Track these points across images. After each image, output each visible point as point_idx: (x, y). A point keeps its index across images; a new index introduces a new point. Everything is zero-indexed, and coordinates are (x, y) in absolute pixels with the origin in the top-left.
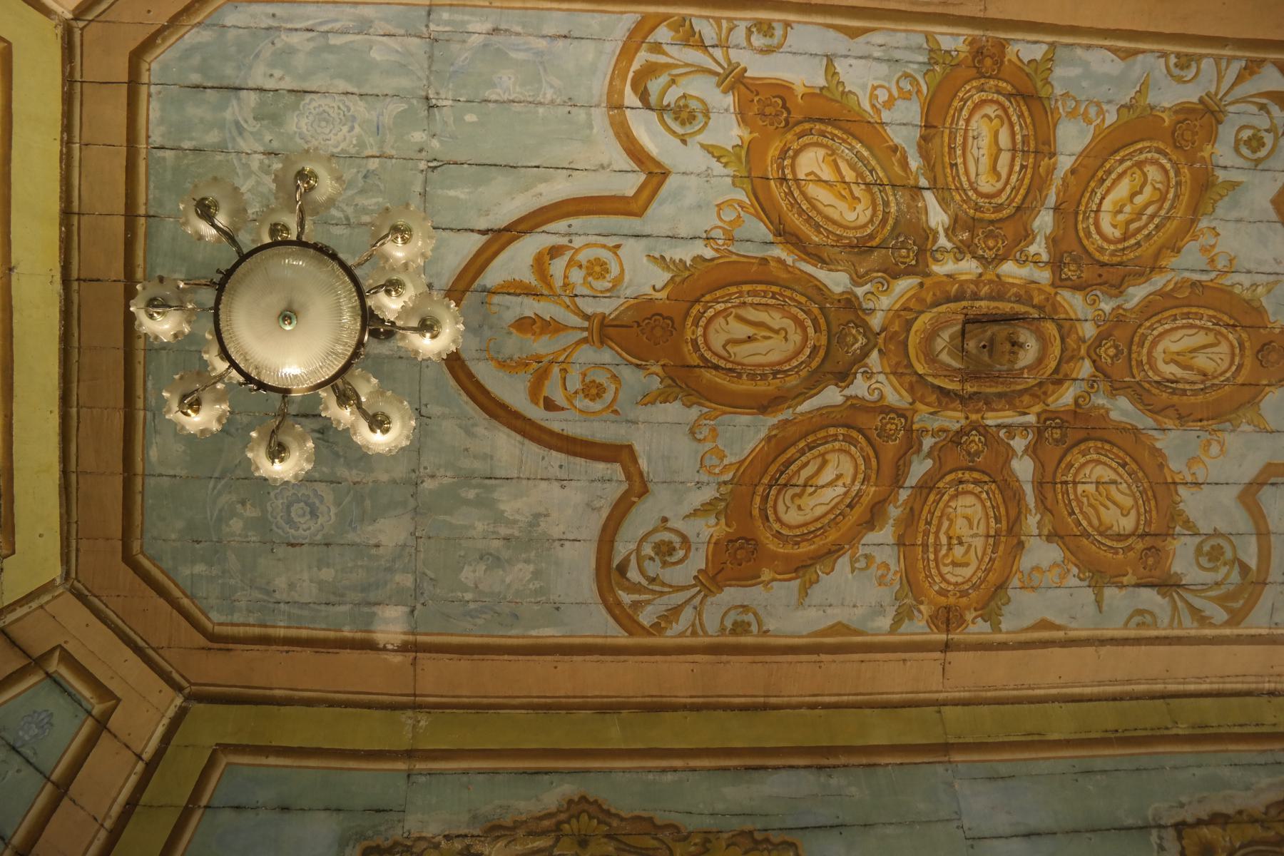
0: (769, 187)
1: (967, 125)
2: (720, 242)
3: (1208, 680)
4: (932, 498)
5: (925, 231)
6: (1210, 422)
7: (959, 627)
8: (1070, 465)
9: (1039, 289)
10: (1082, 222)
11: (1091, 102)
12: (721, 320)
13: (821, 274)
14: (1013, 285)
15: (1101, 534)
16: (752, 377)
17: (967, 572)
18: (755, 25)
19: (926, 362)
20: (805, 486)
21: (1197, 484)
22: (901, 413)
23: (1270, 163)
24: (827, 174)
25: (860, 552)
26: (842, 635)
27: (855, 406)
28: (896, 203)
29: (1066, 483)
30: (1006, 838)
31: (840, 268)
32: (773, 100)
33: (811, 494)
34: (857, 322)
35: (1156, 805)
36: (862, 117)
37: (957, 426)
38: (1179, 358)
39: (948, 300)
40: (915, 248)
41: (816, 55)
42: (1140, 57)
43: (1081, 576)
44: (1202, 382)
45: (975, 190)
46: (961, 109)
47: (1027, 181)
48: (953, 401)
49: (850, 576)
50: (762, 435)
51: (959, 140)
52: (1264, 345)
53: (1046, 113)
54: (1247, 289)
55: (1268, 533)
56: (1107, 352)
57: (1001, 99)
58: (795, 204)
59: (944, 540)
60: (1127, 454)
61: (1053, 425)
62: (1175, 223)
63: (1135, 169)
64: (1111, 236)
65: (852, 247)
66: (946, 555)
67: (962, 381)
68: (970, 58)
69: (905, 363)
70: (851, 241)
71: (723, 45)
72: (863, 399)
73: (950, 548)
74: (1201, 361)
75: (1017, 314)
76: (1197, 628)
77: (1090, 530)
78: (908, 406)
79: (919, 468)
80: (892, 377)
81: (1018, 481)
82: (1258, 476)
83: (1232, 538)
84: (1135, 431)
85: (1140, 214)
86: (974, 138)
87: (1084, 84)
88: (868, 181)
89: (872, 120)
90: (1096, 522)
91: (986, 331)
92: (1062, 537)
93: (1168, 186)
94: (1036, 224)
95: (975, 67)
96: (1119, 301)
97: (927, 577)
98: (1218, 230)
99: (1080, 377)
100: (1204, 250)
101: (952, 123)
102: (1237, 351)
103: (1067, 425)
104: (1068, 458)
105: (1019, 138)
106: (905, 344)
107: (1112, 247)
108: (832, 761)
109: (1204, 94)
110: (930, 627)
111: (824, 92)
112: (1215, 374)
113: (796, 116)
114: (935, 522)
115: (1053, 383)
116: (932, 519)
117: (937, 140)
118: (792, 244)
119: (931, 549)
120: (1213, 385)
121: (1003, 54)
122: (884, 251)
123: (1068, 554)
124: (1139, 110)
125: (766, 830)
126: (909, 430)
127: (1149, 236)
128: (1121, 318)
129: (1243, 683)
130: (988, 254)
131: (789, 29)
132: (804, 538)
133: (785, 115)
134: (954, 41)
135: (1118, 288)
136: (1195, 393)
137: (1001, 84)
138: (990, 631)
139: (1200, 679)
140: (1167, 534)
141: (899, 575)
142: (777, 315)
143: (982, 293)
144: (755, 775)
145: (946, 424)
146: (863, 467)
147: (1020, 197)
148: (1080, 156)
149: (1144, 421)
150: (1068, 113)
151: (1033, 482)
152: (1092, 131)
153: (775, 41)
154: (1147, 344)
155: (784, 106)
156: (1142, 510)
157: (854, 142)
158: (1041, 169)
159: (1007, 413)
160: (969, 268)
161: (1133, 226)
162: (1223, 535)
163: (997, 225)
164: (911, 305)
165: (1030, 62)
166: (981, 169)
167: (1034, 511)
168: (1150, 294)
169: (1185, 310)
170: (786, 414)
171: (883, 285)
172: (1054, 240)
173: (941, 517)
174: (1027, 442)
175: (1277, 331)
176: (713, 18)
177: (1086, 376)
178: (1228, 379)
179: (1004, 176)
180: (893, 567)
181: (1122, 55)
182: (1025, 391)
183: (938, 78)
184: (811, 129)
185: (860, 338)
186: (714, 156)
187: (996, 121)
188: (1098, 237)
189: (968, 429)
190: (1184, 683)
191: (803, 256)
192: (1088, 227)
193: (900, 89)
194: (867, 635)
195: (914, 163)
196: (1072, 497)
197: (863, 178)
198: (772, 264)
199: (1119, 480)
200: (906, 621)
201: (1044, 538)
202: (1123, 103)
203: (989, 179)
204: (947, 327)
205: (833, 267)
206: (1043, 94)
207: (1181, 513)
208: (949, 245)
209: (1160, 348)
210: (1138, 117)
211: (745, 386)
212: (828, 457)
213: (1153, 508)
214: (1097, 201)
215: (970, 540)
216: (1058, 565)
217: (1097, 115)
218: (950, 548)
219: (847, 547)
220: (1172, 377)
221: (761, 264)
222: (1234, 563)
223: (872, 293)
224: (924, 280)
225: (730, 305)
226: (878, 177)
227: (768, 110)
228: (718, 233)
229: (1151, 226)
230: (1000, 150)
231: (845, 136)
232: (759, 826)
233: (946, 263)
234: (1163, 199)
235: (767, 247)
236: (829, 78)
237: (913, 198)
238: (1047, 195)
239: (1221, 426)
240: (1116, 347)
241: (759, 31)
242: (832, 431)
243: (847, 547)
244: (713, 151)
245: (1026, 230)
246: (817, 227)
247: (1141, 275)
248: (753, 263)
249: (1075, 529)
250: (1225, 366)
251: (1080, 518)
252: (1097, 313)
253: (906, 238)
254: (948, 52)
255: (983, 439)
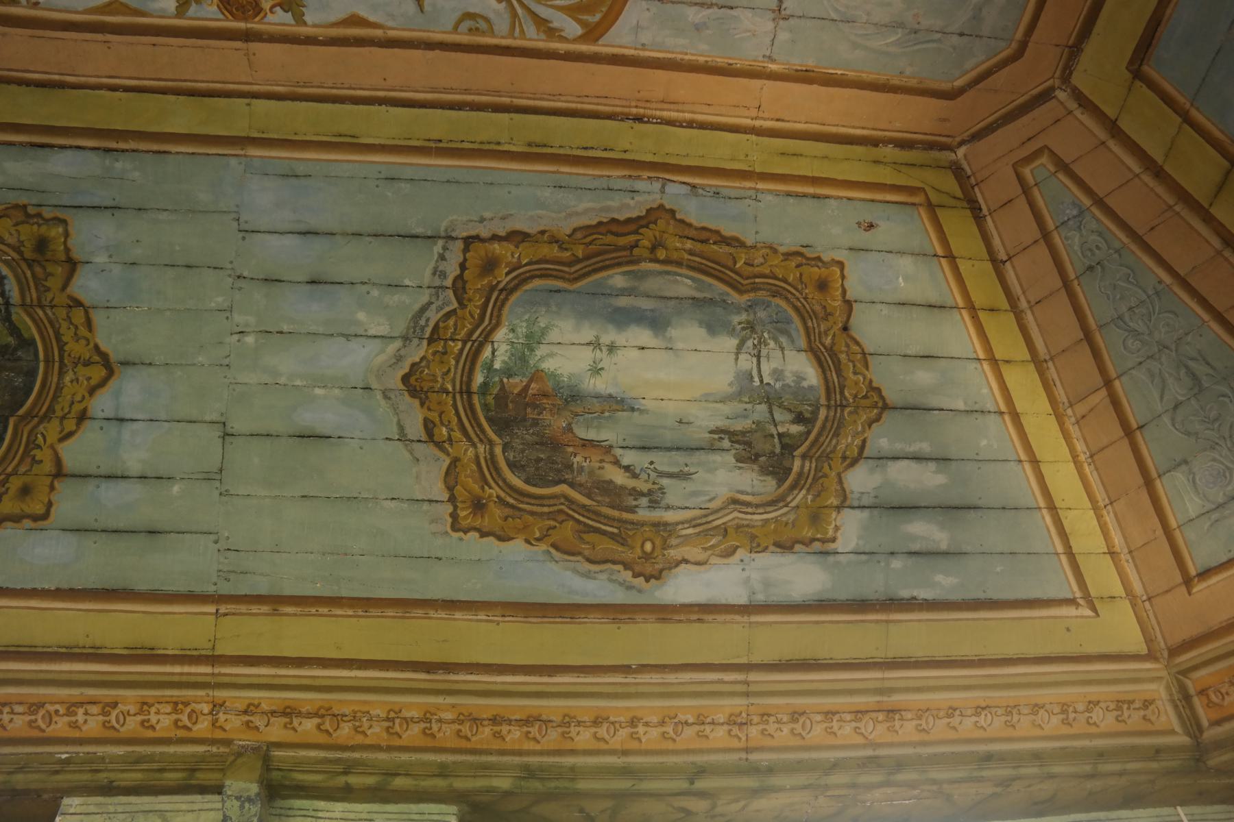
3: (563, 98)
7: (256, 15)
26: (124, 14)
30: (281, 233)
35: (455, 217)
76: (543, 40)
108: (122, 145)
110: (223, 14)
125: (40, 206)
129: (605, 105)
138: (293, 22)
139: (553, 96)
144: (40, 152)
190: (534, 99)
194: (151, 16)
200: (194, 4)
232: (34, 201)
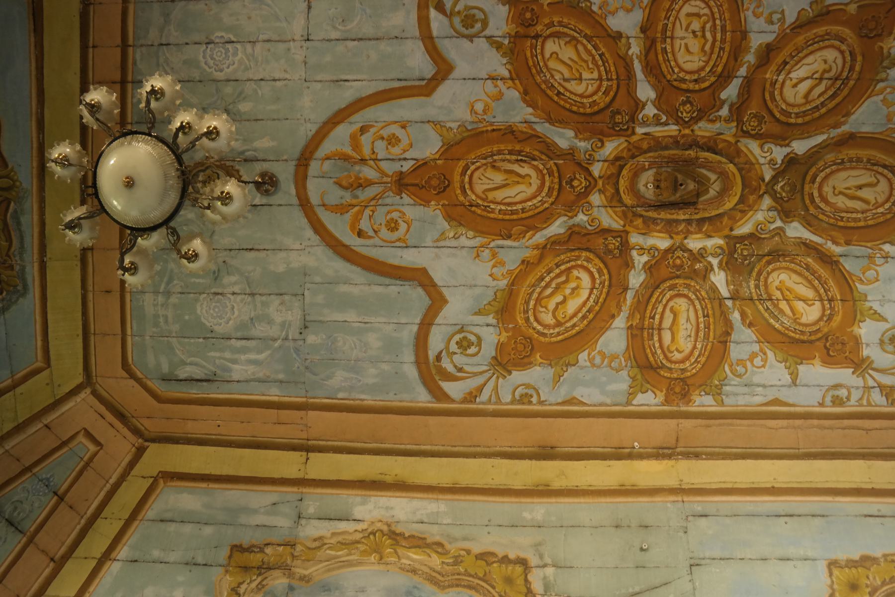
0: (841, 294)
1: (695, 345)
2: (878, 255)
4: (720, 69)
5: (729, 269)
6: (485, 129)
8: (606, 93)
9: (638, 229)
10: (605, 280)
11: (599, 367)
12: (880, 200)
13: (807, 235)
14: (660, 232)
15: (574, 38)
16: (859, 160)
17: (687, 9)
18: (844, 403)
19: (727, 172)
20: (821, 79)
21: (492, 78)
22: (747, 134)
23: (451, 330)
24: (800, 306)
25: (777, 26)
27: (782, 139)
28: (750, 287)
29: (608, 80)
31: (793, 240)
32: (835, 354)
33: (817, 72)
34: (781, 201)
36: (773, 346)
37: (702, 124)
38: (517, 179)
39: (710, 219)
40: (736, 256)
41: (803, 386)
42: (560, 400)
43: (589, 4)
44: (495, 161)
45: (690, 299)
46: (699, 356)
47: (650, 307)
48: (705, 143)
49: (785, 7)
50: (853, 117)
51: (701, 334)
52: (444, 191)
53: (634, 357)
54: (462, 234)
55: (422, 40)
56: (580, 183)
57: (668, 365)
58: (823, 284)
59: (708, 35)
60: (557, 103)
61: (621, 125)
62: (528, 283)
63: (563, 321)
64: (581, 270)
65: (783, 255)
66: (707, 22)
67: (697, 158)
68: (691, 392)
69: (743, 172)
70: (784, 258)
71: (867, 388)
72: (776, 145)
73: (703, 29)
74: (499, 178)
75: (655, 211)
77: (585, 41)
78: (741, 140)
79: (731, 92)
80: (754, 161)
81: (649, 82)
82: (437, 86)
83: (456, 35)
84: (551, 121)
85: (558, 288)
86: (690, 336)
87: (604, 379)
88: (770, 302)
89: (766, 344)
90: (580, 48)
91: (680, 197)
92: (609, 36)
93: (534, 309)
94: (642, 277)
95: (688, 385)
96: (571, 222)
97: (721, 6)
98: (491, 279)
99: (601, 164)
100: (502, 264)
101: (707, 345)
102: (467, 186)
103: (610, 126)
104: (608, 99)
105: (656, 338)
106: (744, 186)
107: (579, 262)
109: (508, 377)
111: (799, 361)
112: (485, 167)
113: (820, 344)
114: (717, 50)
115: (623, 158)
116: (719, 52)
117: (718, 333)
118: (827, 255)
119: (719, 28)
120: (485, 158)
121: (666, 396)
122: (760, 253)
123: (602, 22)
124: (561, 362)
126: (740, 122)
127: (549, 272)
128: (567, 208)
130: (679, 253)
131: (821, 402)
132: (822, 38)
133: (828, 344)
134: (703, 402)
135: (574, 232)
136: (500, 152)
137: (669, 375)
140: (516, 38)
141: (745, 7)
142: (840, 205)
143: (683, 225)
145: (710, 126)
146: (776, 93)
147: (655, 296)
148: (609, 327)
149: (544, 129)
150: (617, 357)
151: (636, 81)
152: (598, 347)
153: (831, 393)
154: (546, 189)
155: (828, 350)
156: (539, 57)
157: (780, 328)
158: (639, 317)
159: (660, 134)
160: (695, 243)
161: (563, 278)
162: (464, 36)
163: (674, 275)
164: (739, 215)
165: (647, 391)
166: (685, 315)
167: (634, 57)
168: (545, 228)
169: (515, 217)
170: (834, 133)
171: (761, 228)
172: (628, 266)
173: (712, 53)
174: (644, 112)
175: (433, 203)
176: (873, 406)
177: (596, 164)
178: (473, 163)
179: (668, 311)
180: (749, 13)
181: (575, 401)
182: (645, 152)
183: (716, 376)
184: (810, 335)
185: (779, 190)
186: (879, 314)
187: (673, 348)
188: (592, 269)
189: (691, 122)
191: (819, 247)
192: (600, 277)
193: (745, 367)
195: (736, 316)
196: (602, 68)
197: (773, 304)
198: (842, 241)
199: (562, 82)
201: (624, 35)
202: (573, 368)
203: (679, 308)
204: (711, 199)
205: (798, 240)
206: (636, 370)
207: (504, 55)
208: (710, 259)
209: (534, 188)
210: (562, 358)
211: (864, 153)
212: (803, 101)
213: (530, 59)
214: (593, 296)
215: (686, 35)
216: (610, 12)
217: (594, 358)
218: (703, 29)
219: (788, 31)
220: (522, 164)
221: (850, 241)
222: (451, 14)
223: (769, 222)
224: (729, 233)
225: (874, 211)
226: (762, 305)
227: (839, 347)
228: (879, 261)
229: (547, 279)
230: (670, 329)
231: (786, 332)
233: (712, 246)
234: (538, 301)
235: (845, 253)
236: (795, 371)
237: (737, 291)
238: (634, 299)
239: (475, 126)
240: (572, 187)
241: (842, 399)
242: (800, 121)
243: (788, 31)
244: (879, 317)
245: (651, 272)
246: (808, 268)
247: (554, 243)
248: (856, 241)
249: (598, 42)
250: (476, 175)
251: (594, 51)
252: (590, 212)
253: (743, 263)
254: (707, 394)
255: (680, 114)
